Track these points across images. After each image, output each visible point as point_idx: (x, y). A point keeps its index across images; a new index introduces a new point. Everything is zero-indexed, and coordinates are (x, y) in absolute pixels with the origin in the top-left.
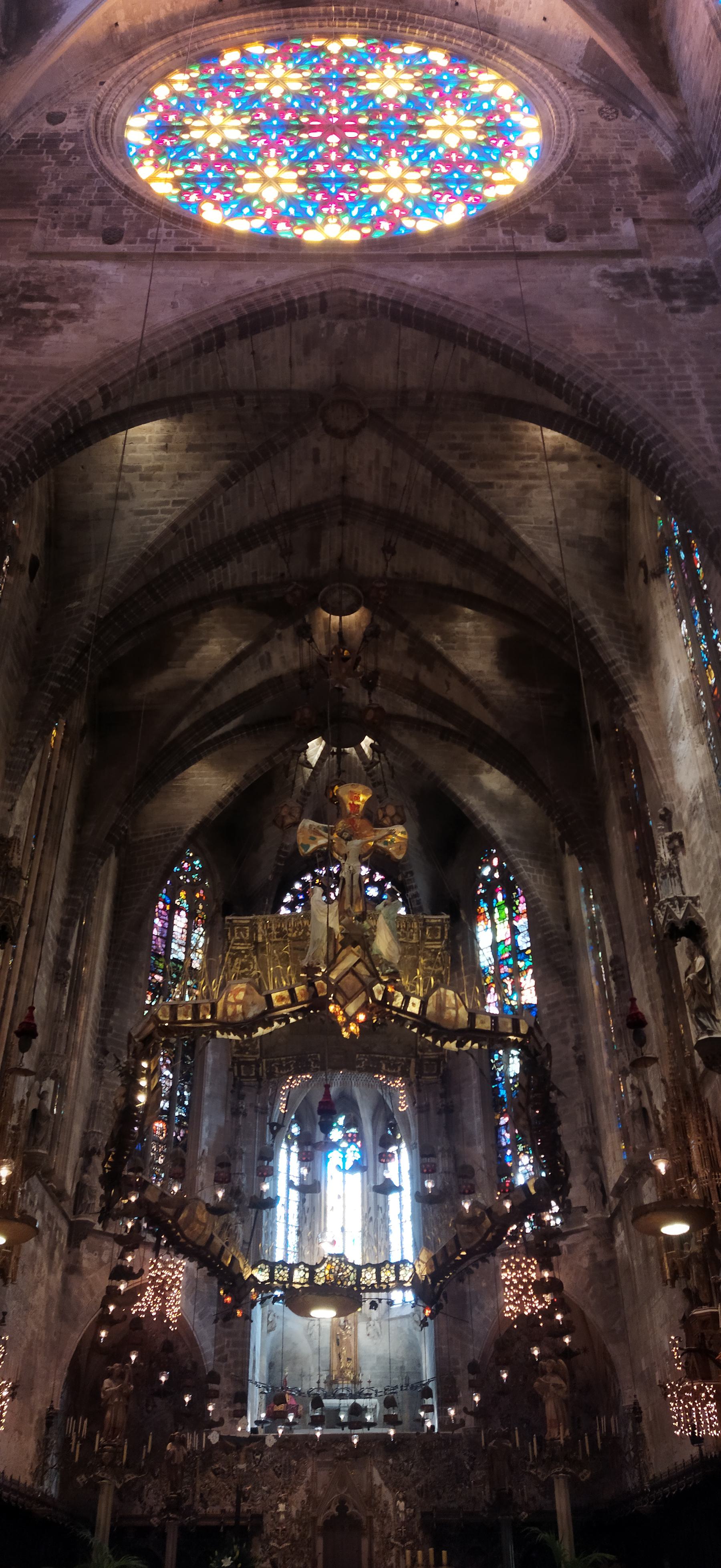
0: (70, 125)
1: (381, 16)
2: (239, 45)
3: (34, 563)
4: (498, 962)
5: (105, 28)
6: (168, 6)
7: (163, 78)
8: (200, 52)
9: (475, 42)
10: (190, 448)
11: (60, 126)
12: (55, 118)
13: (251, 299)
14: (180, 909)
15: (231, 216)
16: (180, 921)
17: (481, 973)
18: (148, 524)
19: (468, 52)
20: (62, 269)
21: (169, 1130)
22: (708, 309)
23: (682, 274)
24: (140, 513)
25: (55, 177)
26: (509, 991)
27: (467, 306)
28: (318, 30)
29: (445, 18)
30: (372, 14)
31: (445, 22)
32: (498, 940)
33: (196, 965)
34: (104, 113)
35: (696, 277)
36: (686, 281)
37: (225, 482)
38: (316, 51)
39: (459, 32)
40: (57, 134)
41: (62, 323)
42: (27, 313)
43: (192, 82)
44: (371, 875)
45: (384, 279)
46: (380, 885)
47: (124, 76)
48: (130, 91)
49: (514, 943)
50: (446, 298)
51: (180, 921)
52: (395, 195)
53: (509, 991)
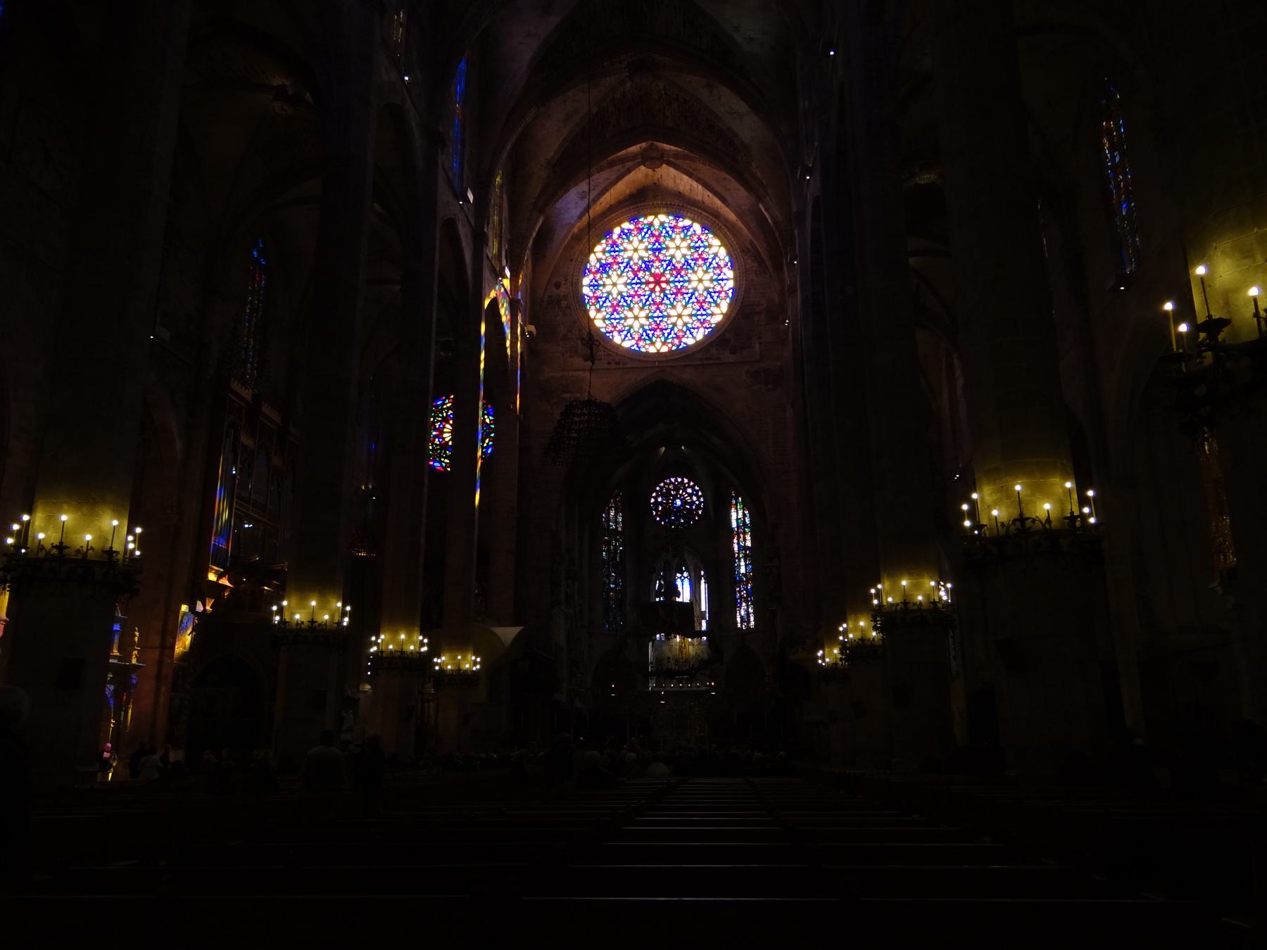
0: (563, 290)
4: (738, 526)
11: (560, 290)
12: (558, 286)
14: (613, 507)
16: (612, 514)
17: (732, 529)
21: (615, 596)
26: (741, 539)
31: (700, 211)
32: (739, 517)
33: (620, 529)
43: (604, 252)
44: (689, 483)
46: (693, 487)
48: (582, 262)
49: (744, 520)
51: (612, 514)
53: (741, 539)
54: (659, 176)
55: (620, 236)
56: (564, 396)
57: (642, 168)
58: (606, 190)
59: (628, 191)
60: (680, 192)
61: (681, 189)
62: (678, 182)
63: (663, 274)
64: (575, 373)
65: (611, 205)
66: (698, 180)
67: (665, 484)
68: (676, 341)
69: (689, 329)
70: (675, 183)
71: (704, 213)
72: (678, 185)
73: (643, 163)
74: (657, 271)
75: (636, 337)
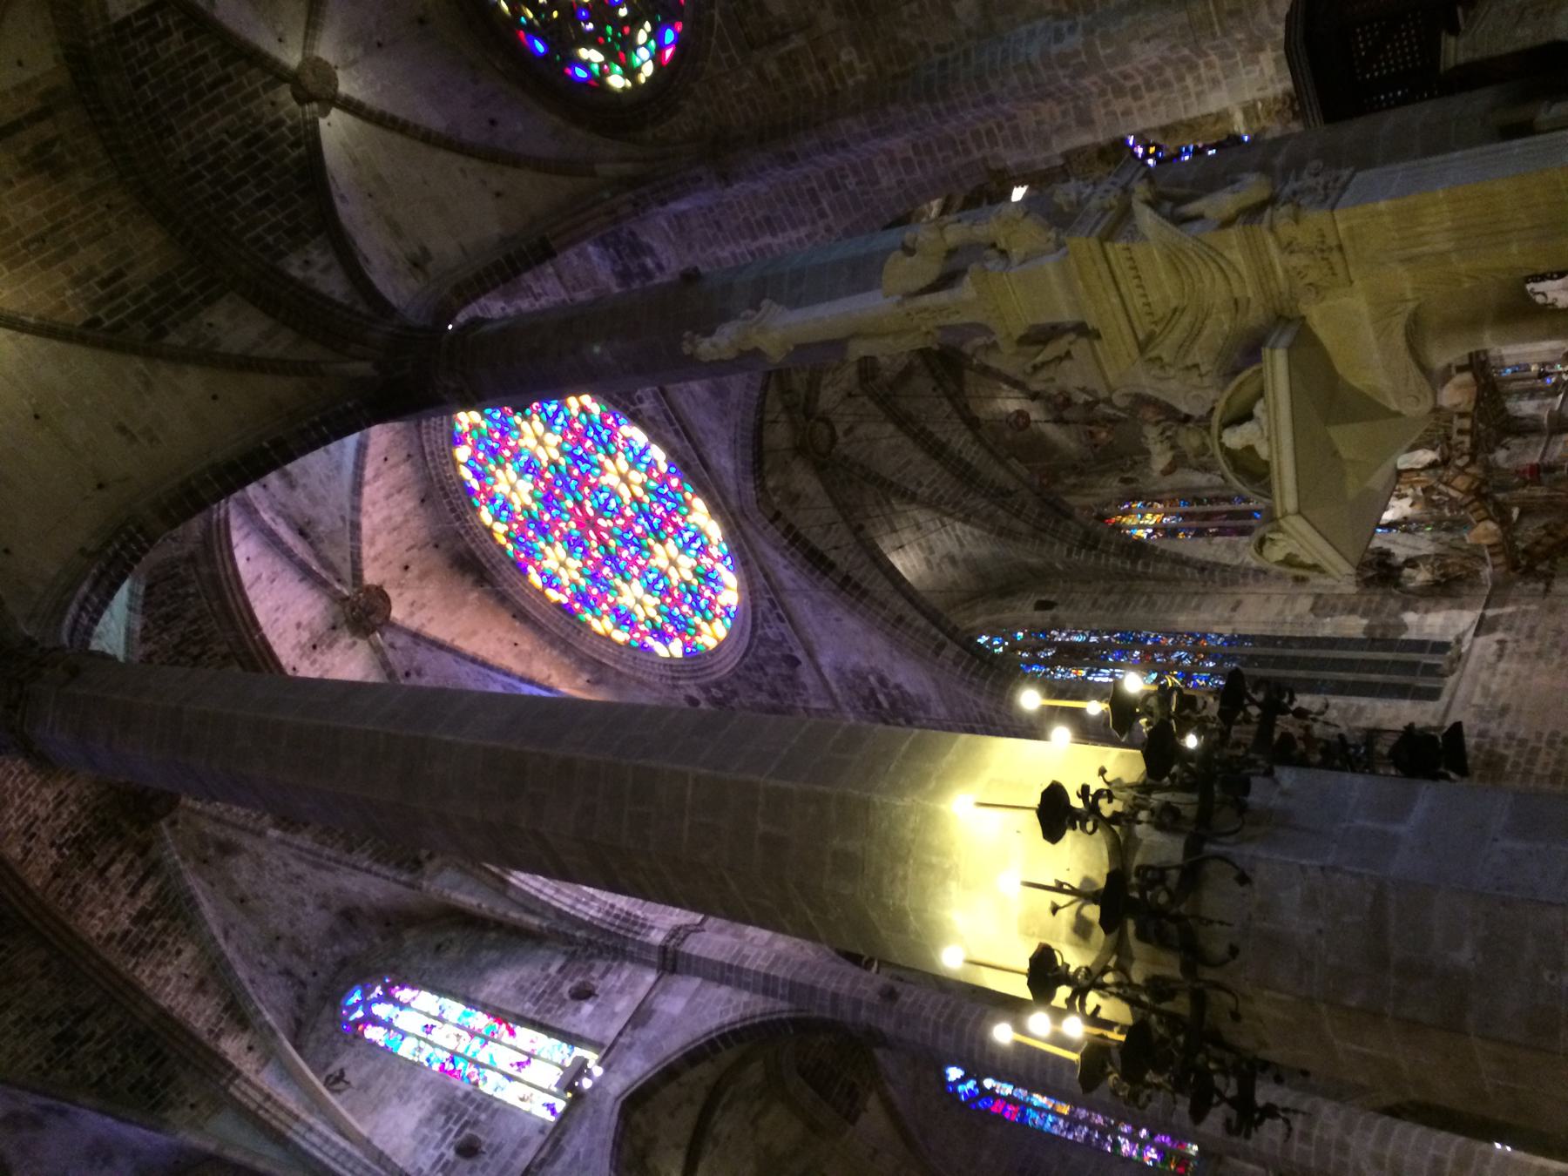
0: (694, 692)
1: (450, 503)
2: (541, 593)
3: (1043, 606)
5: (597, 688)
6: (548, 651)
7: (607, 638)
8: (565, 617)
9: (432, 432)
10: (894, 531)
12: (693, 702)
13: (805, 571)
15: (722, 584)
18: (969, 537)
19: (445, 433)
20: (841, 688)
22: (645, 239)
23: (614, 262)
24: (962, 545)
25: (752, 697)
27: (736, 426)
28: (490, 542)
29: (425, 458)
30: (453, 510)
31: (429, 458)
34: (669, 673)
35: (611, 250)
36: (621, 258)
37: (912, 498)
38: (514, 541)
39: (430, 446)
40: (707, 699)
41: (891, 685)
42: (893, 704)
45: (738, 485)
47: (624, 665)
50: (735, 442)
52: (637, 477)
54: (415, 551)
55: (559, 588)
56: (885, 705)
57: (397, 614)
58: (474, 660)
59: (473, 596)
60: (423, 501)
61: (409, 505)
62: (399, 519)
63: (571, 511)
64: (833, 685)
65: (514, 616)
66: (357, 509)
67: (1146, 155)
68: (674, 482)
69: (638, 458)
70: (406, 521)
71: (427, 450)
72: (406, 515)
73: (388, 623)
74: (573, 525)
75: (706, 561)
